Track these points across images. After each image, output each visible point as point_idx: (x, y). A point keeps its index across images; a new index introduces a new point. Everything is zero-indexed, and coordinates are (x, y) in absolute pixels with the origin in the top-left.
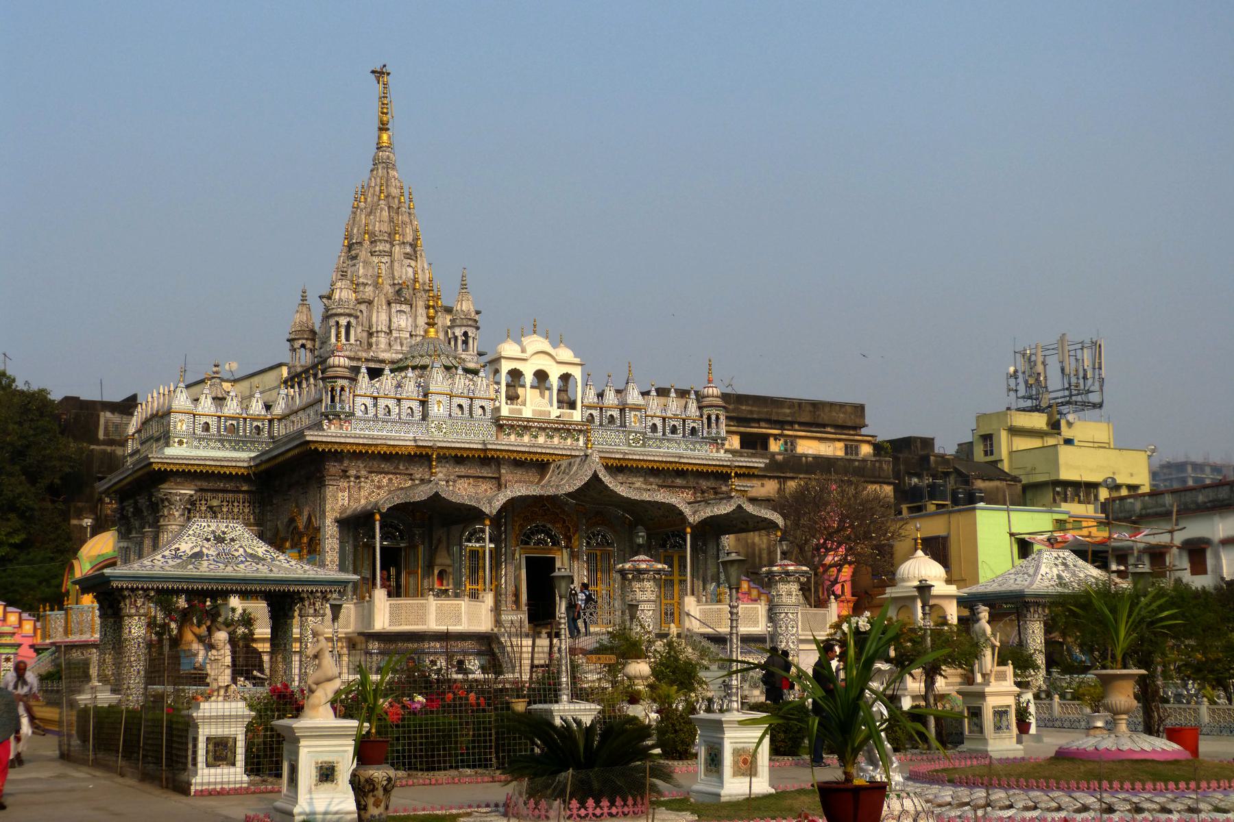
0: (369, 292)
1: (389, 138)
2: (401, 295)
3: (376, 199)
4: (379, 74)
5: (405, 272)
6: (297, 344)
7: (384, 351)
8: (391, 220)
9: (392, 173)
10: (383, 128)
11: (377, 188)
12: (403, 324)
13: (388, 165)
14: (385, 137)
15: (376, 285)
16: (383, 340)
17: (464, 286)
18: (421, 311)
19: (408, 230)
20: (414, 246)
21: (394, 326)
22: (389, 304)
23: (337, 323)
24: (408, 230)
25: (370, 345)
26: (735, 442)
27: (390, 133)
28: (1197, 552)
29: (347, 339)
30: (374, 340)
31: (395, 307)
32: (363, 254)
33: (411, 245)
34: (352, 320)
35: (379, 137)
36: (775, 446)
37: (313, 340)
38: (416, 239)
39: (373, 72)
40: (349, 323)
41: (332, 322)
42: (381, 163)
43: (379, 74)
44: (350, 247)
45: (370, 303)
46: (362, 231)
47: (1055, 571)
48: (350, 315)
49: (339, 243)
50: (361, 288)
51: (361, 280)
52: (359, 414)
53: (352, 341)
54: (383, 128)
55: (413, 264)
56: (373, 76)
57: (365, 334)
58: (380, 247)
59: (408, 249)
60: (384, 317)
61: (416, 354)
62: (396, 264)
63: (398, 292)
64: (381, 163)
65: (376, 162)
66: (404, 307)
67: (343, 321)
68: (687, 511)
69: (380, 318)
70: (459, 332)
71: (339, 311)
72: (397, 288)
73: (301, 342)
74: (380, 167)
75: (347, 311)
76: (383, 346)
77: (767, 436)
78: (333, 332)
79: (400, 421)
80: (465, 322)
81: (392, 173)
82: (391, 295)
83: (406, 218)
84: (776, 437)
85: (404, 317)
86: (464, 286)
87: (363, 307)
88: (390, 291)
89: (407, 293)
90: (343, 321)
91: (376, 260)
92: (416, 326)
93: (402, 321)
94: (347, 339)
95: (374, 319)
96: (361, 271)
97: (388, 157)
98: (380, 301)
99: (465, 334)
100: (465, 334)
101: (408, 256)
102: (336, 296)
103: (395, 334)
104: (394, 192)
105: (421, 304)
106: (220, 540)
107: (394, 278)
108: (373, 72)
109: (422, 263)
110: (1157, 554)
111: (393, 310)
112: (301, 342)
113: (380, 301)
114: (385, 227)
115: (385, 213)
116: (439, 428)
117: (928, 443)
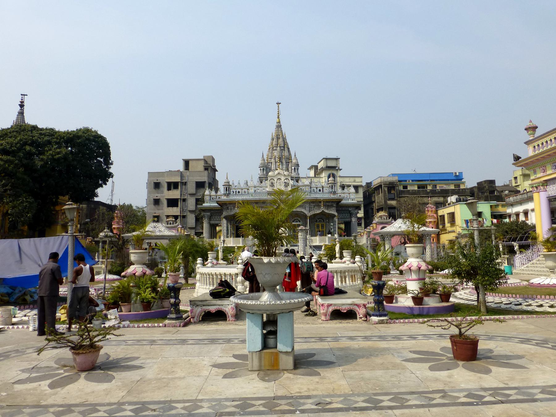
26: (416, 188)
28: (526, 213)
36: (429, 188)
42: (279, 126)
43: (278, 104)
47: (400, 225)
52: (232, 193)
64: (279, 126)
68: (306, 212)
70: (293, 168)
77: (426, 185)
79: (242, 194)
84: (429, 185)
106: (155, 227)
110: (517, 215)
116: (252, 195)
117: (493, 182)
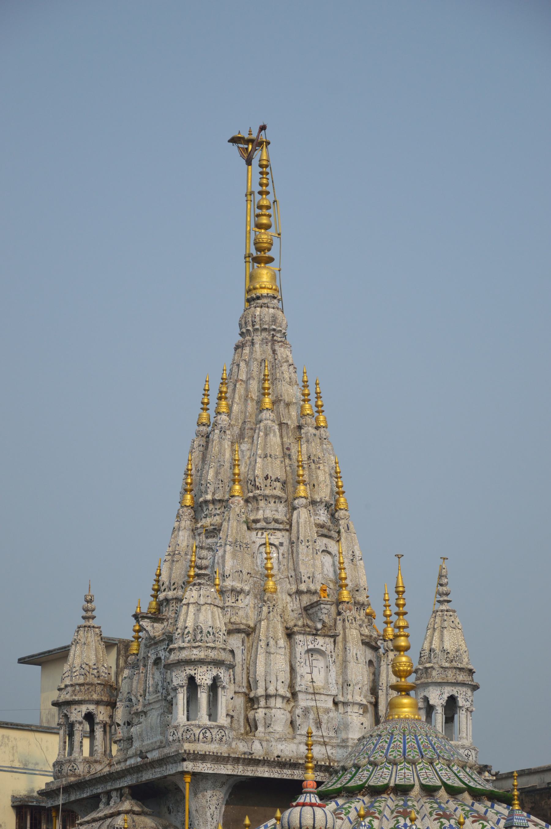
0: (246, 610)
1: (274, 278)
2: (316, 616)
3: (251, 407)
4: (249, 145)
5: (318, 568)
6: (77, 714)
7: (278, 742)
8: (286, 454)
9: (282, 352)
10: (260, 257)
11: (254, 385)
12: (319, 678)
13: (275, 336)
14: (265, 275)
15: (262, 595)
16: (279, 713)
17: (443, 598)
18: (358, 653)
19: (323, 476)
20: (333, 509)
21: (301, 684)
22: (290, 635)
23: (191, 679)
24: (323, 476)
25: (252, 726)
27: (273, 266)
29: (212, 715)
30: (260, 714)
31: (303, 643)
32: (233, 528)
33: (328, 506)
34: (223, 674)
35: (252, 277)
37: (113, 705)
38: (338, 493)
39: (234, 140)
40: (215, 679)
41: (179, 678)
43: (249, 145)
44: (198, 508)
45: (249, 632)
46: (226, 473)
48: (218, 663)
49: (168, 498)
50: (230, 601)
51: (229, 583)
53: (223, 720)
54: (260, 257)
55: (332, 546)
56: (234, 148)
57: (240, 701)
58: (269, 511)
59: (323, 517)
60: (280, 663)
61: (379, 757)
62: (302, 548)
63: (308, 610)
65: (247, 330)
66: (321, 643)
67: (204, 677)
69: (272, 667)
71: (197, 654)
72: (306, 600)
73: (84, 709)
74: (258, 338)
75: (213, 655)
76: (280, 727)
78: (181, 698)
80: (450, 676)
81: (282, 352)
82: (293, 618)
83: (315, 449)
85: (320, 663)
86: (443, 598)
87: (235, 642)
88: (291, 606)
89: (327, 613)
90: (204, 677)
91: (258, 538)
92: (346, 684)
93: (317, 674)
94: (212, 715)
95: (260, 669)
96: (229, 564)
97: (274, 319)
98: (272, 629)
99: (452, 701)
100: (452, 701)
101: (324, 532)
102: (188, 619)
103: (304, 701)
104: (291, 392)
105: (353, 634)
107: (299, 580)
108: (234, 140)
109: (349, 545)
111: (300, 649)
112: (84, 709)
113: (272, 629)
114: (277, 470)
115: (275, 439)
